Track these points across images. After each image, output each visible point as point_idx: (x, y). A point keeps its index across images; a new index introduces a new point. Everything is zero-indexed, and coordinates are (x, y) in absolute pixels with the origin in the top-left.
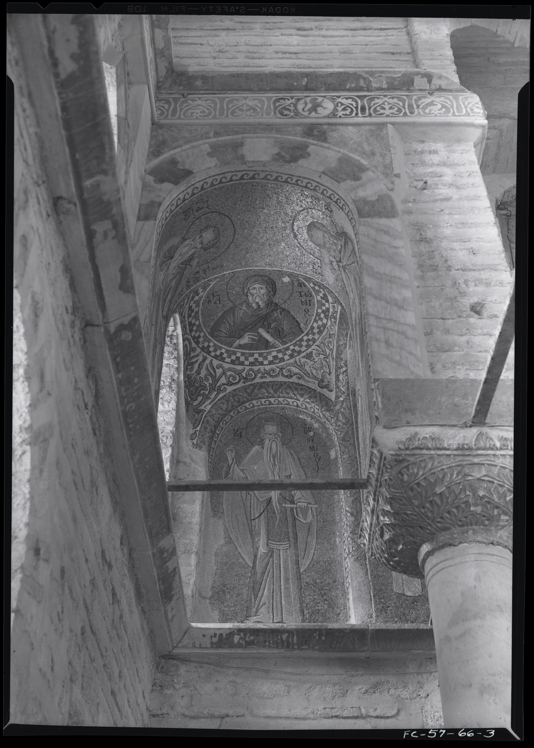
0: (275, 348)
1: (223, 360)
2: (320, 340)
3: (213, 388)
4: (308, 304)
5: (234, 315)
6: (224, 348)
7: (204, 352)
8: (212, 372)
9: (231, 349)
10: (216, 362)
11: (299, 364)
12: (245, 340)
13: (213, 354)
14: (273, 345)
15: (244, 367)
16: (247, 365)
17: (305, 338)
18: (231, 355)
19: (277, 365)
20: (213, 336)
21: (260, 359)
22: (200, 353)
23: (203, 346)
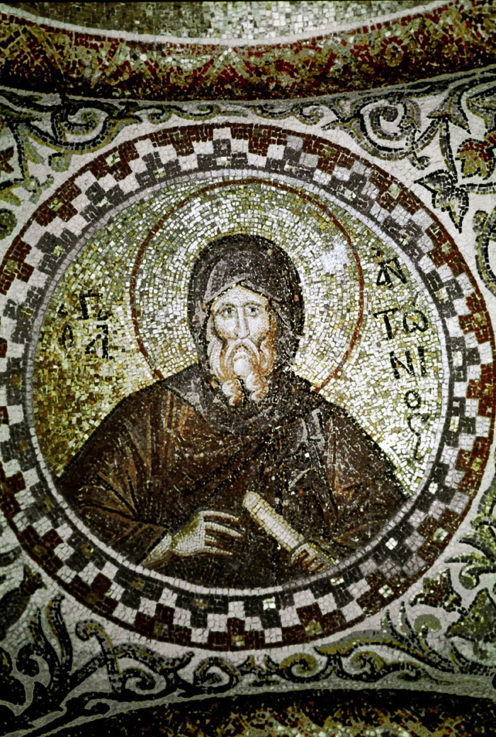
0: (306, 574)
1: (107, 608)
2: (472, 515)
3: (45, 700)
4: (417, 370)
5: (156, 424)
6: (114, 562)
7: (34, 557)
8: (54, 642)
9: (139, 569)
10: (75, 612)
11: (398, 629)
12: (193, 542)
13: (67, 574)
14: (300, 561)
15: (187, 649)
17: (417, 519)
18: (138, 594)
19: (319, 643)
20: (68, 498)
21: (253, 624)
23: (30, 529)
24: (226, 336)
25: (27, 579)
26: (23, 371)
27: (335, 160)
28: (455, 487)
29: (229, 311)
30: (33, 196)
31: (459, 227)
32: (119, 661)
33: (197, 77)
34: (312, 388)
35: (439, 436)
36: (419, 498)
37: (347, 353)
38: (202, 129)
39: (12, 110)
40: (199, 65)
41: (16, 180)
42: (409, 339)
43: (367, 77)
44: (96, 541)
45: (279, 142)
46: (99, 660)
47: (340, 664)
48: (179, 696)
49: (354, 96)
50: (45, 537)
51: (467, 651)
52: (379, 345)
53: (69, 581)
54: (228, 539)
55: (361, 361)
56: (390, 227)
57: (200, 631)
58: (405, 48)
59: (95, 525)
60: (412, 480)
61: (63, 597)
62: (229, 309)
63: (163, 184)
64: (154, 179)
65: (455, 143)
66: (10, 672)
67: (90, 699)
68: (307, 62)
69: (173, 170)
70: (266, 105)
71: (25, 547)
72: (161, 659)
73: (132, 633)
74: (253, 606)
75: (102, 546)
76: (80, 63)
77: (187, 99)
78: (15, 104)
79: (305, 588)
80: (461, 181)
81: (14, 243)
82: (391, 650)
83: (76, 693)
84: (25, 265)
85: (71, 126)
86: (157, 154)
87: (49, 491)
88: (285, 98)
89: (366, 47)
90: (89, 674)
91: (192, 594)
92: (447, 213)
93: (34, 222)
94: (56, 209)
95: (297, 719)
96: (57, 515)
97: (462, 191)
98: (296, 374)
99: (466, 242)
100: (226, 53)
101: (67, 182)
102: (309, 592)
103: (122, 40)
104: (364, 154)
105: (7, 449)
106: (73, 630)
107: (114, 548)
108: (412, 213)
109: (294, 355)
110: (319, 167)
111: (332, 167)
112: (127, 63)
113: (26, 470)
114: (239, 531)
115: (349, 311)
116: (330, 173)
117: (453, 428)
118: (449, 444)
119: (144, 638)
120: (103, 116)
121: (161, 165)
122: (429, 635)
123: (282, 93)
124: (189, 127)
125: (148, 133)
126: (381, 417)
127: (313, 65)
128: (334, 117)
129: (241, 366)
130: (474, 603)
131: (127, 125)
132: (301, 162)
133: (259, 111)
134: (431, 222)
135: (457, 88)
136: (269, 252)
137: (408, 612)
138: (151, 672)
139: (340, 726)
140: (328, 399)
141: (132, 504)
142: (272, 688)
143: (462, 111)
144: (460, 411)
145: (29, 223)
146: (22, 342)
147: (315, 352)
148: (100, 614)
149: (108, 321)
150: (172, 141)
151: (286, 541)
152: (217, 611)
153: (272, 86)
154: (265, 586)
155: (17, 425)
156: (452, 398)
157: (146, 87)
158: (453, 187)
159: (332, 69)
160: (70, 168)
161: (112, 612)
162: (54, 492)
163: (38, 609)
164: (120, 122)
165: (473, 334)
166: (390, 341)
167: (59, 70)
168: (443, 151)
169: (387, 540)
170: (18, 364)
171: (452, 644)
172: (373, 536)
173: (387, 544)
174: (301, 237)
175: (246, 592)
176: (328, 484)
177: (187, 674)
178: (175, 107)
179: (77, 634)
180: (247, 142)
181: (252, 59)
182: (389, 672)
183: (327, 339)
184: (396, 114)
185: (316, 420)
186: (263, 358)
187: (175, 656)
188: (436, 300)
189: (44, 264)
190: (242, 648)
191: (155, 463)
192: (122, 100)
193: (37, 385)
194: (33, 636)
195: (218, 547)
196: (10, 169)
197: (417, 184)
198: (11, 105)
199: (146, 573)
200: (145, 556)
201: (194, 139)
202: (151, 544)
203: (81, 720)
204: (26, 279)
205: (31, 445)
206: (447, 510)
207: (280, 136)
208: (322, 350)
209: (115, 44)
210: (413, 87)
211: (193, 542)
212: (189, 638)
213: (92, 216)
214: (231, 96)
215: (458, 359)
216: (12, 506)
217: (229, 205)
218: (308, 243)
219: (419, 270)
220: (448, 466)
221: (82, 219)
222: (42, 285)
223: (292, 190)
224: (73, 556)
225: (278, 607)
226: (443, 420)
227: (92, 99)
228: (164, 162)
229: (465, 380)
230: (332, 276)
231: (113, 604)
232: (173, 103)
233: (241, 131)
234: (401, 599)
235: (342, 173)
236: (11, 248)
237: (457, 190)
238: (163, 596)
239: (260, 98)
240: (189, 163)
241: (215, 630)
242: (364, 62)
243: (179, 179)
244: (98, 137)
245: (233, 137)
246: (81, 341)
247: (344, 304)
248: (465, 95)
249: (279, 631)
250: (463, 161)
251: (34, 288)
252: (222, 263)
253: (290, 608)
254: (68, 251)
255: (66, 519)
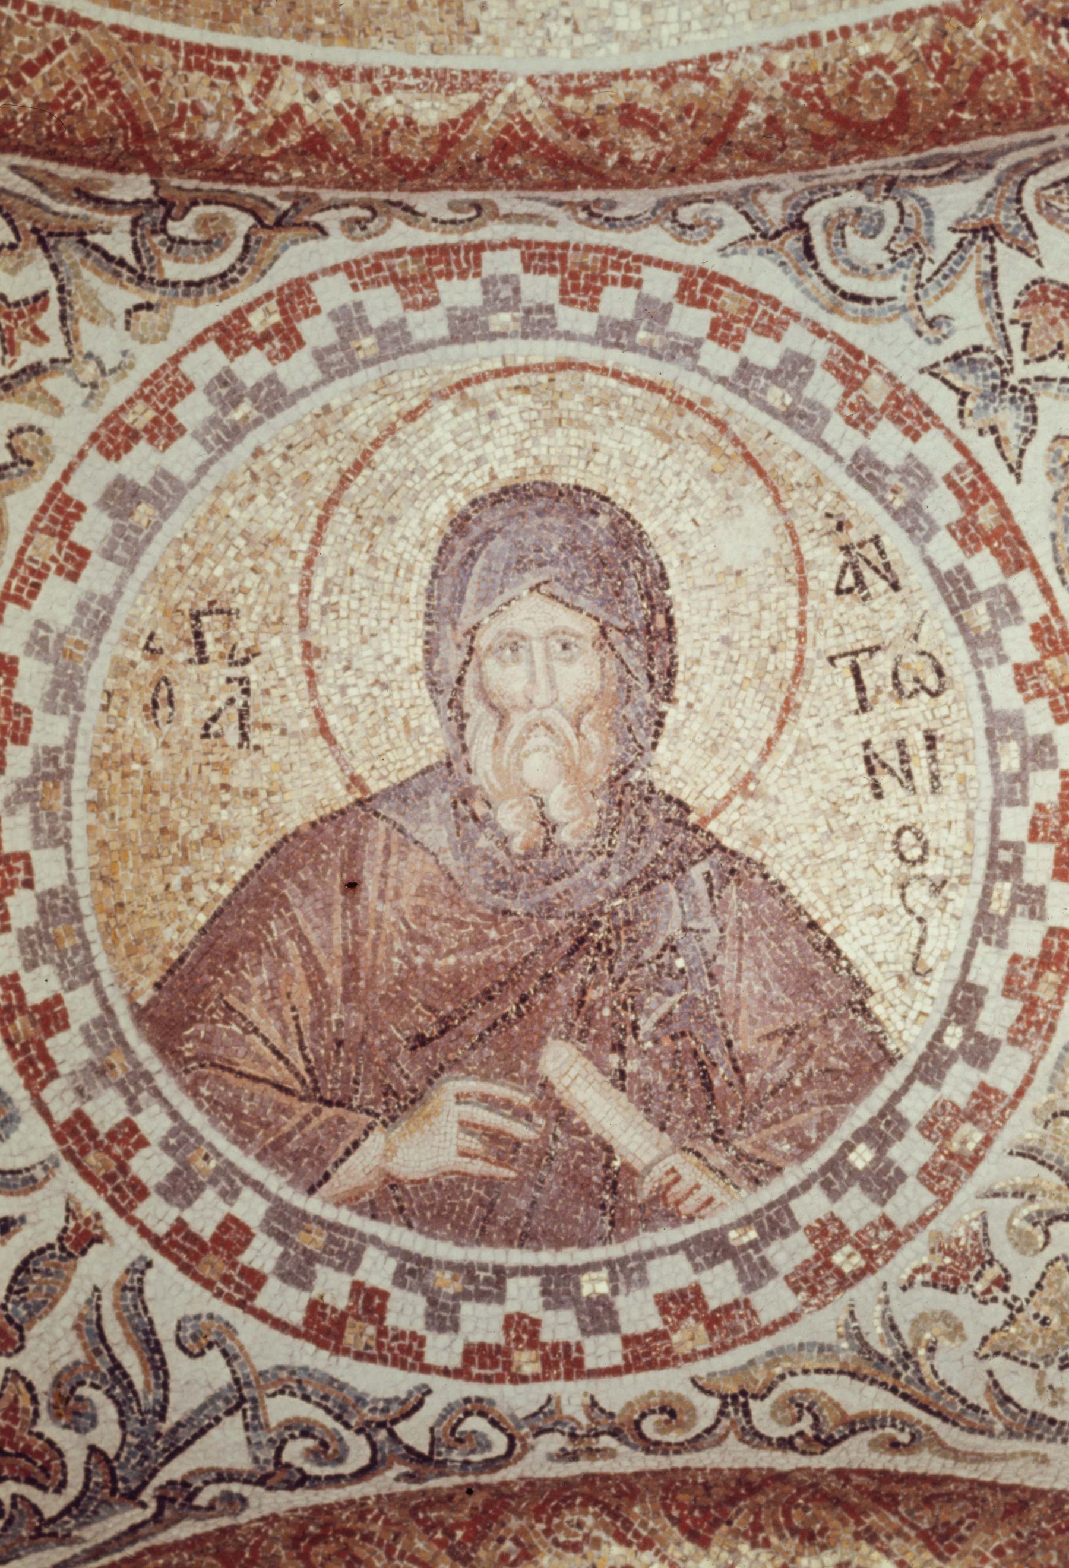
0: (674, 1218)
2: (1037, 1096)
3: (110, 1483)
4: (921, 779)
6: (259, 1187)
7: (87, 1176)
8: (131, 1361)
9: (313, 1205)
11: (873, 1341)
12: (431, 1145)
13: (158, 1214)
14: (661, 1195)
16: (446, 1372)
17: (917, 1104)
18: (311, 1258)
19: (702, 1368)
21: (560, 1326)
22: (49, 1167)
24: (506, 703)
25: (72, 1224)
26: (66, 774)
27: (748, 321)
28: (1002, 1035)
29: (514, 648)
30: (91, 396)
31: (1015, 470)
32: (268, 1402)
33: (447, 139)
34: (693, 819)
35: (967, 924)
36: (923, 1058)
37: (769, 742)
38: (457, 252)
39: (46, 209)
40: (453, 114)
41: (54, 361)
42: (904, 713)
43: (819, 142)
44: (221, 1143)
45: (627, 282)
46: (227, 1400)
47: (747, 1413)
48: (397, 1479)
49: (791, 182)
50: (111, 1135)
51: (1021, 1386)
52: (838, 724)
53: (161, 1229)
54: (507, 1143)
55: (798, 760)
56: (866, 470)
57: (444, 1339)
58: (900, 80)
59: (215, 1108)
60: (908, 1020)
61: (149, 1265)
62: (515, 643)
63: (373, 372)
64: (352, 359)
65: (1010, 287)
66: (34, 1422)
67: (207, 1483)
68: (687, 110)
69: (396, 341)
70: (597, 202)
71: (69, 1154)
72: (360, 1400)
73: (300, 1342)
74: (558, 1285)
75: (233, 1153)
76: (196, 108)
77: (427, 188)
78: (53, 196)
79: (673, 1250)
80: (1021, 371)
81: (50, 498)
82: (857, 1384)
83: (176, 1470)
84: (72, 546)
85: (175, 243)
86: (359, 306)
87: (120, 1036)
88: (642, 185)
89: (816, 78)
90: (203, 1431)
91: (428, 1261)
92: (990, 439)
93: (93, 454)
94: (139, 426)
95: (653, 1531)
96: (136, 1085)
97: (1024, 391)
98: (658, 786)
99: (1031, 504)
100: (510, 88)
101: (164, 367)
102: (681, 1257)
103: (286, 60)
104: (810, 310)
105: (31, 944)
106: (172, 1336)
107: (260, 1157)
108: (916, 437)
109: (654, 745)
110: (711, 336)
111: (740, 337)
112: (296, 109)
113: (71, 987)
114: (532, 1126)
115: (774, 650)
116: (736, 349)
117: (998, 907)
118: (988, 941)
119: (324, 1354)
120: (243, 222)
121: (369, 331)
122: (939, 1355)
123: (631, 175)
124: (431, 249)
125: (341, 260)
126: (841, 882)
127: (700, 114)
128: (747, 229)
129: (538, 768)
130: (1039, 1285)
131: (295, 242)
132: (673, 325)
133: (583, 215)
134: (958, 458)
135: (1017, 167)
136: (603, 520)
137: (894, 1304)
138: (339, 1427)
139: (744, 1548)
140: (727, 842)
141: (301, 1066)
142: (599, 1466)
143: (1024, 218)
144: (1013, 870)
145: (82, 455)
146: (65, 713)
147: (700, 738)
148: (229, 1300)
149: (250, 668)
150: (394, 278)
151: (632, 1148)
152: (481, 1296)
153: (612, 160)
154: (585, 1244)
155: (52, 893)
156: (996, 844)
157: (337, 160)
158: (1004, 384)
159: (741, 125)
160: (171, 335)
161: (252, 1297)
162: (132, 1035)
163: (96, 1289)
164: (279, 236)
165: (1043, 703)
166: (864, 717)
167: (149, 124)
168: (984, 304)
169: (852, 1148)
170: (55, 760)
171: (990, 1373)
172: (821, 1139)
173: (852, 1157)
174: (672, 489)
175: (547, 1257)
176: (724, 1027)
177: (415, 1433)
178: (399, 204)
179: (179, 1342)
180: (555, 281)
181: (569, 102)
182: (853, 1432)
183: (726, 710)
184: (882, 221)
185: (701, 887)
186: (587, 753)
187: (390, 1394)
188: (963, 628)
189: (113, 545)
190: (536, 1378)
191: (351, 976)
192: (286, 189)
193: (95, 805)
194: (85, 1346)
195: (486, 1160)
196: (40, 337)
197: (926, 377)
198: (45, 199)
199: (329, 1213)
200: (327, 1177)
201: (440, 275)
202: (340, 1153)
203: (185, 1530)
204: (74, 577)
205: (81, 934)
206: (984, 1087)
207: (628, 268)
208: (714, 734)
209: (271, 68)
210: (922, 164)
211: (431, 1145)
212: (420, 1356)
213: (219, 440)
214: (520, 180)
215: (1011, 759)
216: (41, 1066)
217: (515, 419)
218: (687, 501)
219: (929, 563)
220: (985, 990)
221: (196, 447)
222: (108, 590)
223: (653, 387)
224: (174, 1175)
225: (615, 1291)
226: (977, 890)
227: (220, 186)
228: (375, 322)
229: (1024, 802)
230: (739, 573)
231: (255, 1279)
232: (395, 196)
233: (542, 257)
234: (881, 1275)
235: (762, 351)
236: (43, 509)
237: (1013, 389)
238: (366, 1263)
239: (585, 187)
240: (429, 324)
241: (476, 1339)
242: (813, 108)
243: (405, 360)
244: (232, 268)
245: (527, 269)
246: (192, 710)
247: (765, 634)
248: (1033, 184)
249: (614, 1342)
250: (1027, 326)
251: (92, 596)
252: (498, 544)
253: (638, 1294)
254: (165, 516)
255: (157, 1093)
